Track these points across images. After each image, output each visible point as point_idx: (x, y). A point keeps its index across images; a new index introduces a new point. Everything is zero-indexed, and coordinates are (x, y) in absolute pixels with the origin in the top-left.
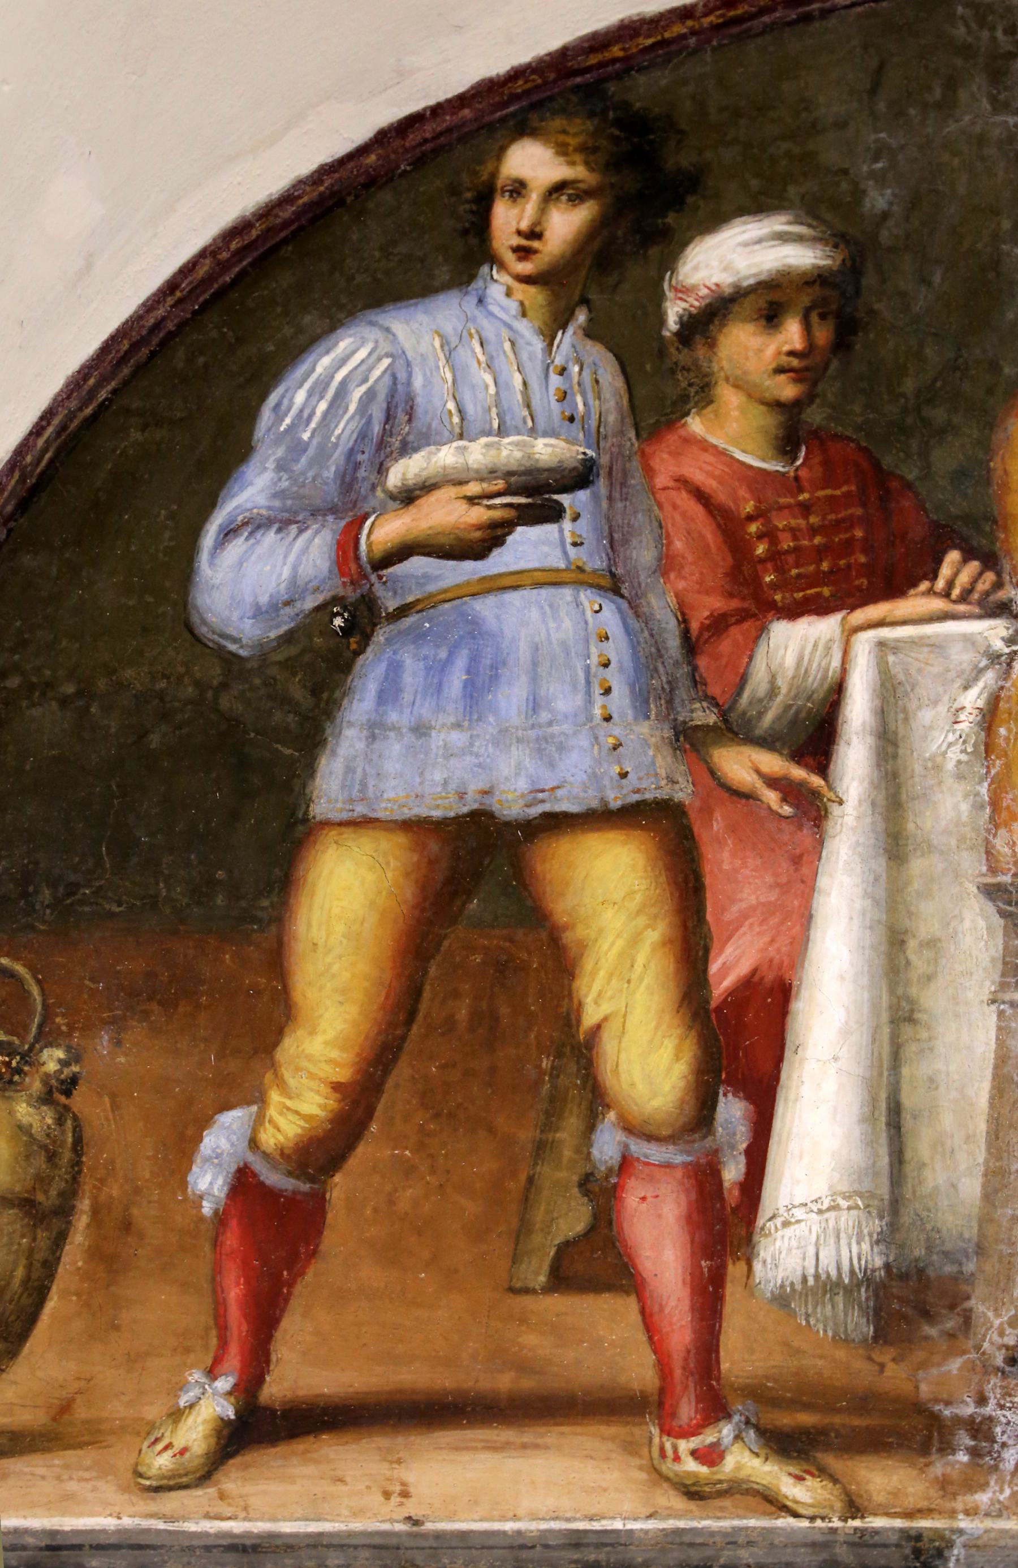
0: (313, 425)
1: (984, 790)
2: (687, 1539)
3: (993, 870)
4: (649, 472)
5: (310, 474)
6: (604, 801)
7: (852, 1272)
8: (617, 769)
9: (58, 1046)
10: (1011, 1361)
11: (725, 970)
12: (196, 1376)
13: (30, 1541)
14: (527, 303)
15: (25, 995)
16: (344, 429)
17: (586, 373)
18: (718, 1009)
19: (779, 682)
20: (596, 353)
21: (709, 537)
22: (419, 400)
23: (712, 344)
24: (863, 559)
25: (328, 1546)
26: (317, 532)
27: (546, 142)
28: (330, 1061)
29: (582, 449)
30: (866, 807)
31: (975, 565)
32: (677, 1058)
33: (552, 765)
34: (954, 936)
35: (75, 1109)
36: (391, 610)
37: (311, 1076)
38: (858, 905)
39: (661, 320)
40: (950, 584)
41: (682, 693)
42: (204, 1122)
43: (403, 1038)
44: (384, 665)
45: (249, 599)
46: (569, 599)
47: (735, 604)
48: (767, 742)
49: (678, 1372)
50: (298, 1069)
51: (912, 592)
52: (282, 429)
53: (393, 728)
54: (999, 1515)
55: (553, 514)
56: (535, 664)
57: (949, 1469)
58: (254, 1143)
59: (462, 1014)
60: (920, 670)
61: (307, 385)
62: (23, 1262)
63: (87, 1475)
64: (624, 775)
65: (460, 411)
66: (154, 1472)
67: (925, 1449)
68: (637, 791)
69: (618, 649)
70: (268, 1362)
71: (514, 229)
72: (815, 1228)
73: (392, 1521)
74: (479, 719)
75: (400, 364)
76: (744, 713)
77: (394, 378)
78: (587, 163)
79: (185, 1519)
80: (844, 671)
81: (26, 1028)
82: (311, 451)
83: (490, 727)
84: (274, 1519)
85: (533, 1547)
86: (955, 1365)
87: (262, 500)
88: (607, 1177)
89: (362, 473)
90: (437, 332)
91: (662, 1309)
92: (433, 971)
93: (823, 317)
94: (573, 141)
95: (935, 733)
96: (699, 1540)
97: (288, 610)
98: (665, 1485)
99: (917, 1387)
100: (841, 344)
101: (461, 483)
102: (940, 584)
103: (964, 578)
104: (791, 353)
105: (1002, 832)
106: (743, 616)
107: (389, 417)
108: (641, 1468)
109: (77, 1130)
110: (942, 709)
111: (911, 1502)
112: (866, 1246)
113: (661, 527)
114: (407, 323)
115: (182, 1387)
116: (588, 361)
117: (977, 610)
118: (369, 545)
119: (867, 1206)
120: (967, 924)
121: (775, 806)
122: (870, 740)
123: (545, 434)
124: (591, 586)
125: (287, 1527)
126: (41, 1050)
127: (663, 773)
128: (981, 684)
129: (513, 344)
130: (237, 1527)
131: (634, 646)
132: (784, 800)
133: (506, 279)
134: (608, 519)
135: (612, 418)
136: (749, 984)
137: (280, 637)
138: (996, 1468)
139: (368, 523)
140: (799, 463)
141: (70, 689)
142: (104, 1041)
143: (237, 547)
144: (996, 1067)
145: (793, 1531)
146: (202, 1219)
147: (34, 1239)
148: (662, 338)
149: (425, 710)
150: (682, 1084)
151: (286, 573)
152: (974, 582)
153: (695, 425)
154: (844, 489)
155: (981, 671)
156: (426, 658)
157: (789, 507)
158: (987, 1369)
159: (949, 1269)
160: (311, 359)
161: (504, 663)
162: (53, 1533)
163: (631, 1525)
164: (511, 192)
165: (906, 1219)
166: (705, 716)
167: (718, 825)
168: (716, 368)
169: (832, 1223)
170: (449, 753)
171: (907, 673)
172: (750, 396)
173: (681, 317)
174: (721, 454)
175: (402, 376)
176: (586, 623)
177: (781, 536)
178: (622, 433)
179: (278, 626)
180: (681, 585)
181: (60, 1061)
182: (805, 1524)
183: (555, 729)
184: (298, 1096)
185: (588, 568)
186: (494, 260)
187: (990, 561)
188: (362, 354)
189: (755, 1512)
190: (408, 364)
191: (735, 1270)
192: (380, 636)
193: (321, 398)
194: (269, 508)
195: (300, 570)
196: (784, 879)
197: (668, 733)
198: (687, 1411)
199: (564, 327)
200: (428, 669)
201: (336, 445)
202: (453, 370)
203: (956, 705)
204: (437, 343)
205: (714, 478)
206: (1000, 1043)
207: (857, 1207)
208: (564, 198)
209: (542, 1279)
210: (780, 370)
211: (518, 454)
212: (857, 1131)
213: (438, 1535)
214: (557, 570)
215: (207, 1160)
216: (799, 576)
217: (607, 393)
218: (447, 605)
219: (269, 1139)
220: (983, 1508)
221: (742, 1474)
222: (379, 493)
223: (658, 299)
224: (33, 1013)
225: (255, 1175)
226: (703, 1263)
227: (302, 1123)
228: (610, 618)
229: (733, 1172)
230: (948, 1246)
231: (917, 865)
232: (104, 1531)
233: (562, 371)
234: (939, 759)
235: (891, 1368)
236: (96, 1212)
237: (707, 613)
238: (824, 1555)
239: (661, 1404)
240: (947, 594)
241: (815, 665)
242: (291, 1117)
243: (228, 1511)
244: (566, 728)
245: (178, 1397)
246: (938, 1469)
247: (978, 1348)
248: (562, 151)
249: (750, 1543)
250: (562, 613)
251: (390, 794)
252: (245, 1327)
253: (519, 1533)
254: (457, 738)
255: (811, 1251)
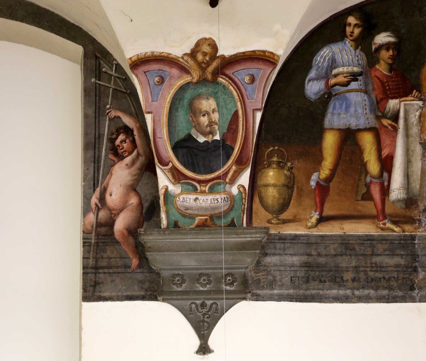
0: (321, 63)
1: (419, 128)
2: (382, 235)
3: (421, 140)
4: (371, 74)
5: (321, 72)
6: (366, 127)
7: (403, 199)
8: (368, 122)
9: (290, 162)
10: (423, 211)
11: (384, 154)
12: (313, 212)
13: (292, 235)
14: (352, 44)
15: (284, 154)
16: (325, 64)
17: (361, 57)
18: (383, 159)
19: (390, 109)
20: (362, 53)
21: (380, 85)
22: (336, 60)
23: (379, 53)
24: (402, 90)
25: (333, 236)
26: (322, 81)
27: (354, 17)
28: (329, 166)
29: (361, 70)
30: (403, 129)
31: (418, 93)
32: (378, 167)
33: (359, 121)
34: (416, 150)
35: (293, 172)
36: (334, 94)
37: (326, 168)
38: (402, 144)
39: (372, 49)
40: (414, 95)
41: (377, 110)
42: (312, 174)
43: (339, 162)
44: (333, 103)
45: (313, 92)
46: (360, 94)
47: (384, 96)
48: (389, 119)
49: (380, 213)
50: (325, 167)
51: (409, 96)
52: (316, 63)
53: (335, 114)
54: (422, 232)
55: (356, 80)
56: (355, 104)
57: (416, 226)
58: (319, 178)
59: (347, 159)
60: (410, 109)
61: (320, 56)
62: (287, 195)
63: (300, 226)
64: (369, 123)
65: (343, 62)
66: (309, 226)
67: (412, 223)
68: (371, 126)
69: (367, 103)
70: (323, 210)
71: (349, 31)
72: (397, 192)
73: (342, 233)
74: (348, 113)
75: (333, 53)
76: (385, 114)
77: (333, 56)
78: (360, 21)
79: (314, 232)
80: (400, 108)
81: (285, 159)
82: (321, 68)
83: (349, 114)
84: (326, 232)
85: (361, 237)
86: (416, 212)
87: (314, 75)
88: (368, 184)
89: (328, 72)
90: (339, 48)
91: (377, 203)
92: (343, 152)
93: (395, 50)
94: (358, 17)
95: (412, 119)
96: (383, 236)
97: (319, 94)
98: (379, 228)
99: (411, 215)
100: (398, 54)
101: (343, 74)
102: (413, 95)
103: (416, 94)
104: (391, 56)
105: (422, 134)
106: (385, 98)
107: (332, 62)
108: (375, 226)
109: (293, 175)
110: (413, 115)
111: (411, 231)
112: (404, 195)
113: (373, 83)
114: (334, 46)
115: (312, 214)
116: (361, 55)
117: (418, 100)
118: (330, 84)
119: (404, 189)
120: (417, 148)
121: (390, 129)
122: (403, 119)
123: (355, 67)
124: (363, 92)
125: (327, 233)
126: (287, 163)
127: (374, 123)
128: (419, 111)
129: (350, 51)
130: (321, 233)
131: (370, 102)
132: (392, 128)
133: (349, 40)
134: (365, 81)
135: (365, 65)
136: (387, 156)
137: (318, 98)
138: (422, 226)
139: (330, 80)
140: (392, 74)
141: (288, 106)
142: (297, 161)
143: (311, 83)
144: (421, 169)
145: (396, 234)
146: (312, 189)
147: (289, 191)
148: (372, 52)
149: (340, 111)
150: (378, 170)
151: (318, 88)
152: (418, 95)
153: (377, 67)
154: (399, 79)
155: (418, 109)
156: (339, 103)
157: (391, 81)
158: (420, 212)
159: (415, 198)
160: (320, 52)
161: (351, 104)
162: (295, 234)
163: (374, 234)
164: (349, 25)
165: (410, 191)
166: (380, 114)
167: (382, 131)
168: (380, 57)
169: (400, 192)
170: (344, 118)
171: (408, 109)
172: (385, 62)
173: (375, 48)
174: (381, 71)
175: (334, 55)
176: (362, 98)
177: (390, 86)
178: (366, 67)
179: (318, 96)
180: (376, 93)
181: (290, 164)
182: (397, 234)
183: (359, 115)
184: (325, 171)
185: (362, 89)
186: (347, 37)
187: (420, 92)
188: (328, 51)
189: (392, 232)
190: (335, 54)
191: (387, 198)
192: (333, 99)
193: (322, 59)
194: (315, 77)
195: (320, 87)
196: (392, 140)
197: (375, 116)
198: (381, 218)
199: (357, 49)
200: (340, 104)
201: (324, 67)
202: (341, 55)
203: (415, 114)
204: (339, 50)
205: (380, 75)
206: (422, 166)
207: (403, 189)
208: (357, 27)
209: (360, 199)
210: (389, 58)
211: (351, 70)
212: (403, 178)
213: (348, 235)
214: (358, 89)
215: (312, 180)
216: (393, 92)
217: (364, 61)
218: (342, 94)
219: (321, 177)
220: (420, 231)
221: (389, 227)
222: (331, 75)
223: (371, 45)
224: (286, 157)
225: (319, 183)
226: (382, 197)
227: (325, 175)
228: (366, 98)
229: (386, 184)
230: (415, 195)
231: (410, 139)
232: (302, 234)
233: (357, 56)
234: (413, 123)
235: (408, 212)
236: (297, 187)
237: (380, 98)
238: (400, 238)
239: (377, 217)
240: (414, 97)
241: (395, 107)
242: (324, 174)
243: (319, 231)
244: (360, 115)
245: (311, 215)
246: (414, 226)
247: (419, 209)
248: (356, 18)
249: (390, 236)
250: (359, 96)
251: (335, 125)
252: (320, 205)
253: (359, 234)
254: (345, 116)
255: (397, 195)
